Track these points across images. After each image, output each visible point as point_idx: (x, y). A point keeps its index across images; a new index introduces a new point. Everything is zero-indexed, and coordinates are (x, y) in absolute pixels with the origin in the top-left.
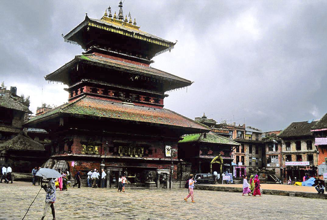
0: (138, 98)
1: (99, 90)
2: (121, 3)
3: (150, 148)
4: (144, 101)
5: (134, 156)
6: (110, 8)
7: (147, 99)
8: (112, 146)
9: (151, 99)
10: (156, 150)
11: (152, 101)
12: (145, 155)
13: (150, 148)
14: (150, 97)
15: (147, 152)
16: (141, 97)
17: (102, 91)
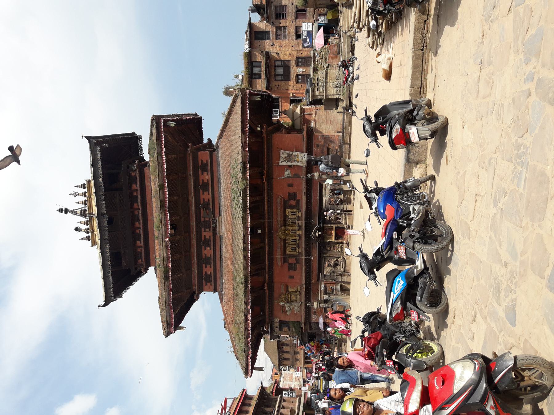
0: (206, 205)
1: (206, 272)
2: (61, 211)
3: (286, 197)
4: (209, 194)
5: (300, 228)
6: (77, 229)
7: (205, 187)
8: (286, 265)
9: (203, 180)
10: (290, 185)
11: (207, 177)
12: (298, 206)
13: (286, 197)
14: (201, 183)
15: (293, 203)
16: (204, 199)
17: (206, 267)
